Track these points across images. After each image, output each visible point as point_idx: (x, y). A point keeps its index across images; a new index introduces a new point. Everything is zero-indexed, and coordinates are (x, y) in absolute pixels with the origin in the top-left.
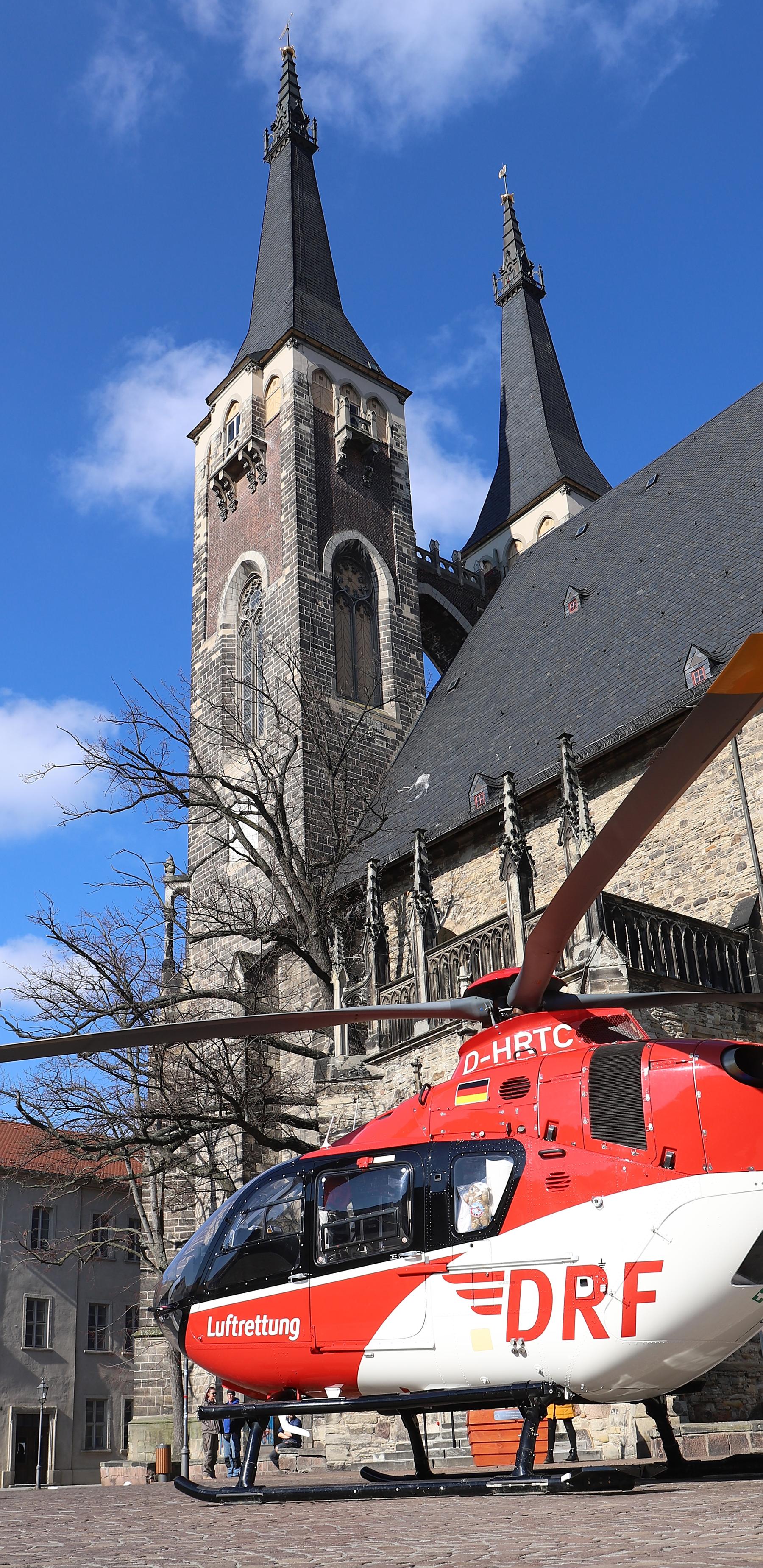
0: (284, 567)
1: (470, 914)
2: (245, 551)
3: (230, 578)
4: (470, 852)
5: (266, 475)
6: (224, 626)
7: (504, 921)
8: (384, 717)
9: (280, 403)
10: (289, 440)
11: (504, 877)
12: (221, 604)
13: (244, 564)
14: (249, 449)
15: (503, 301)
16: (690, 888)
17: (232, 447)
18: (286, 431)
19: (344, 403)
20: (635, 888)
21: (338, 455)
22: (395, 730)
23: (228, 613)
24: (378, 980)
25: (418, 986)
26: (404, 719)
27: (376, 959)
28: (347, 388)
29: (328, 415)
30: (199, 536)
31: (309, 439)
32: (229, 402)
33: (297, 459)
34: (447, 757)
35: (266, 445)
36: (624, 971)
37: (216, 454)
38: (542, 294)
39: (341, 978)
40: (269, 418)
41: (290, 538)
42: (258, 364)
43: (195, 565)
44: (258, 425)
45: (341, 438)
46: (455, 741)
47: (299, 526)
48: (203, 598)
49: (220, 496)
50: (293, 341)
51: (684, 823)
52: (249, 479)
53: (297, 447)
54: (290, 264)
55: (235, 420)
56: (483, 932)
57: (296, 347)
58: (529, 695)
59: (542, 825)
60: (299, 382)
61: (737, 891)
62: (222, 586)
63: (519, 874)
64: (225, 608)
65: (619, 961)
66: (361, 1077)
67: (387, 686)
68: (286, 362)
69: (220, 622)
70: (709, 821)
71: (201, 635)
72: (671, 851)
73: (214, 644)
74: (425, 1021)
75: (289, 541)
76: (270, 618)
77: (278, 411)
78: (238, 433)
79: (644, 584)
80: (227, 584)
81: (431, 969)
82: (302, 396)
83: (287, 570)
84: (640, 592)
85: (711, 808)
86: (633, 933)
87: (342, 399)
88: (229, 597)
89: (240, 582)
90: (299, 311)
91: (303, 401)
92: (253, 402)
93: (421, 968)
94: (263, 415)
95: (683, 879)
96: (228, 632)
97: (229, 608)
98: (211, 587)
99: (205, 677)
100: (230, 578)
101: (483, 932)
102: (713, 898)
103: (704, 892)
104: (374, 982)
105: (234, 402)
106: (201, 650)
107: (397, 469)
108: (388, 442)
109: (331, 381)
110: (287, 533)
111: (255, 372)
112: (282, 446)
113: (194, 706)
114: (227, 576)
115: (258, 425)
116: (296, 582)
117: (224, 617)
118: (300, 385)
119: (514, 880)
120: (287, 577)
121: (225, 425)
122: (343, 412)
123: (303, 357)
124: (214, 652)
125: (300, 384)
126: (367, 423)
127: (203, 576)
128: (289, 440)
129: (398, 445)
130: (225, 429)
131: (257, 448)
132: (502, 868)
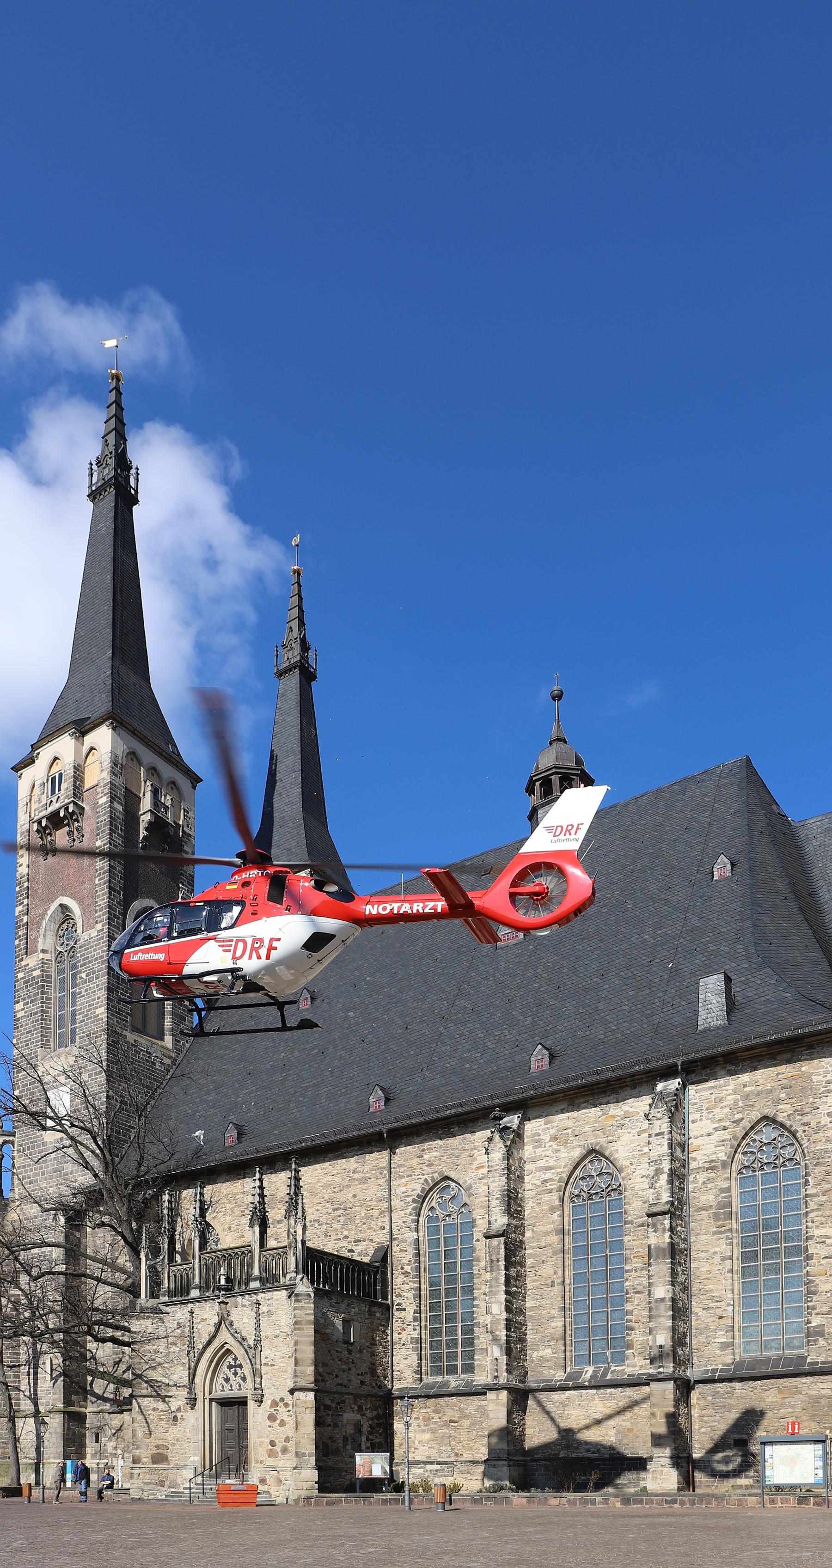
0: (97, 922)
1: (221, 1214)
2: (63, 895)
3: (49, 912)
4: (223, 1177)
5: (83, 836)
6: (43, 951)
7: (249, 1248)
8: (163, 1047)
9: (97, 774)
10: (104, 815)
11: (251, 1225)
12: (42, 932)
13: (61, 905)
14: (70, 810)
15: (281, 675)
16: (353, 1232)
17: (54, 799)
18: (102, 805)
19: (150, 788)
20: (322, 1224)
21: (143, 833)
22: (170, 1058)
23: (46, 940)
24: (169, 1260)
25: (194, 1270)
26: (177, 1048)
27: (168, 1248)
28: (153, 771)
29: (135, 795)
30: (21, 865)
31: (121, 817)
32: (52, 757)
33: (111, 834)
34: (208, 1093)
35: (84, 809)
36: (312, 1295)
37: (40, 801)
38: (313, 677)
39: (147, 1256)
40: (87, 786)
41: (103, 901)
42: (80, 732)
43: (18, 889)
44: (78, 790)
45: (145, 819)
46: (214, 1082)
47: (110, 893)
48: (25, 921)
49: (41, 838)
50: (112, 723)
51: (355, 1196)
52: (70, 833)
53: (111, 824)
54: (109, 630)
55: (57, 775)
56: (235, 1251)
57: (114, 729)
58: (268, 1066)
59: (271, 1173)
60: (115, 763)
61: (378, 1240)
62: (42, 916)
63: (260, 1227)
64: (44, 936)
65: (311, 1290)
66: (157, 1311)
67: (168, 1022)
68: (103, 738)
69: (40, 946)
70: (369, 1199)
71: (23, 951)
72: (345, 1209)
73: (35, 963)
74: (198, 1290)
75: (101, 903)
76: (84, 960)
77: (96, 782)
78: (59, 790)
79: (354, 1009)
80: (47, 918)
81: (203, 1262)
82: (117, 776)
83: (99, 926)
84: (351, 1014)
85: (371, 1192)
86: (318, 1267)
87: (148, 783)
88: (48, 928)
89: (57, 918)
90: (118, 689)
91: (119, 781)
92: (75, 767)
93: (197, 1261)
94: (82, 781)
95: (350, 1226)
96: (47, 956)
97: (48, 937)
98: (32, 913)
99: (26, 987)
100: (49, 912)
101: (235, 1251)
102: (364, 1241)
103: (360, 1237)
104: (166, 1261)
105: (56, 759)
106: (23, 963)
107: (186, 848)
108: (181, 823)
109: (140, 764)
110: (99, 896)
111: (77, 738)
112: (98, 817)
113: (19, 1007)
114: (46, 910)
115: (78, 790)
116: (106, 939)
117: (44, 943)
118: (117, 767)
119: (257, 1229)
120: (99, 931)
121: (48, 777)
122: (148, 795)
123: (119, 740)
124: (35, 970)
125: (116, 765)
126: (166, 808)
127: (26, 901)
128: (104, 815)
129: (188, 826)
130: (48, 780)
131: (77, 811)
132: (251, 1220)
